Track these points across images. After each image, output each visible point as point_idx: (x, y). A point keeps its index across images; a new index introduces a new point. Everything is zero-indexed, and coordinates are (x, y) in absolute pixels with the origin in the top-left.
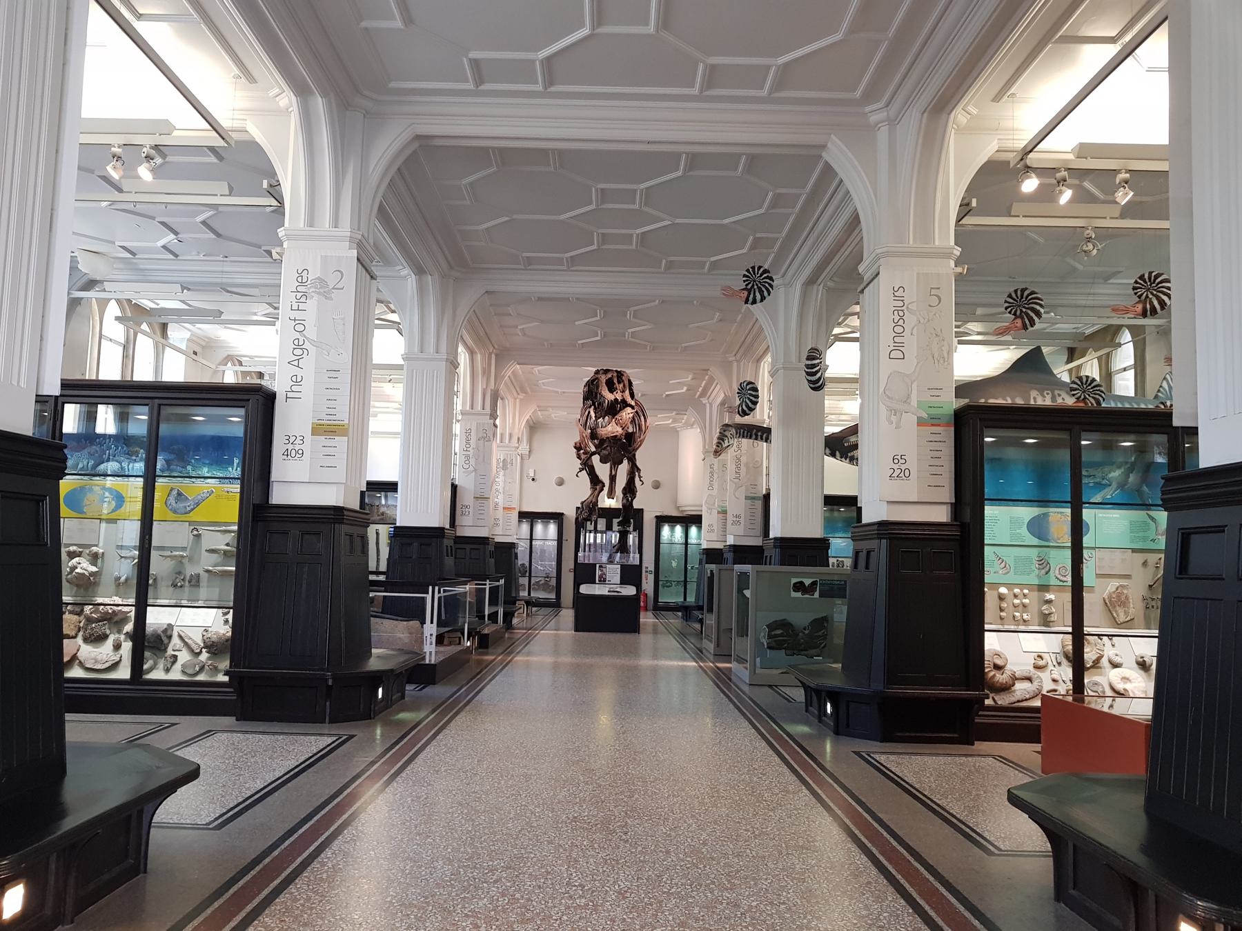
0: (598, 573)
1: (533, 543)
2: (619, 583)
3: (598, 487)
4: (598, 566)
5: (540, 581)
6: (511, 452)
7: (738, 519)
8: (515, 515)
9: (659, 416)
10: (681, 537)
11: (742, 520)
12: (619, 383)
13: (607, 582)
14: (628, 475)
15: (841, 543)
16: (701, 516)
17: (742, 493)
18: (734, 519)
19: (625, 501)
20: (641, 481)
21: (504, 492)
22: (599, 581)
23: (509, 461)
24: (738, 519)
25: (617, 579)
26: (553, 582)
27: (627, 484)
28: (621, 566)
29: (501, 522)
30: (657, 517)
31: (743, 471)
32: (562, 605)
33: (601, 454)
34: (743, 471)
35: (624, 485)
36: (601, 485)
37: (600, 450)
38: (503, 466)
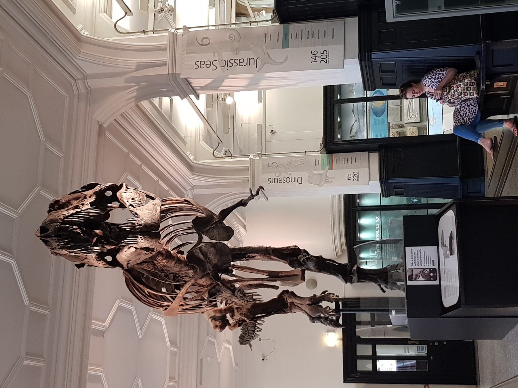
0: (421, 282)
2: (436, 247)
4: (409, 283)
7: (319, 55)
11: (320, 49)
13: (436, 267)
17: (279, 54)
18: (318, 59)
22: (435, 279)
24: (319, 55)
25: (429, 251)
28: (406, 245)
31: (244, 55)
34: (244, 55)
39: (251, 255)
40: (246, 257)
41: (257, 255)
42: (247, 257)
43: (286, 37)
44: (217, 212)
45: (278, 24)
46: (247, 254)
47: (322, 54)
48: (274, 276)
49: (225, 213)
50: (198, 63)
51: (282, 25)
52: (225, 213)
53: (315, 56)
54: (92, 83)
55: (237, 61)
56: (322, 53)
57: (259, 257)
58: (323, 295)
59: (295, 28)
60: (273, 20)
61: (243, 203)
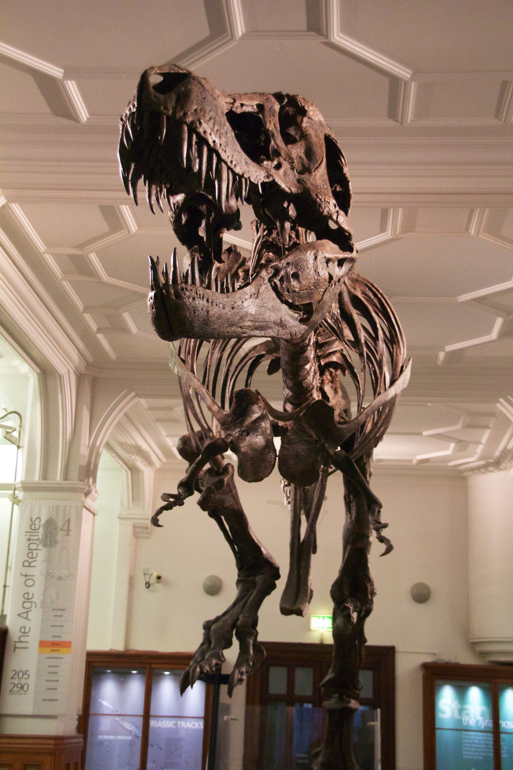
1: (153, 723)
3: (259, 579)
9: (425, 433)
10: (483, 715)
12: (289, 140)
19: (340, 621)
20: (382, 539)
21: (43, 602)
23: (60, 525)
27: (345, 571)
29: (32, 682)
30: (426, 667)
33: (244, 446)
35: (334, 575)
37: (236, 433)
38: (46, 537)
39: (353, 505)
41: (353, 518)
42: (349, 498)
46: (355, 497)
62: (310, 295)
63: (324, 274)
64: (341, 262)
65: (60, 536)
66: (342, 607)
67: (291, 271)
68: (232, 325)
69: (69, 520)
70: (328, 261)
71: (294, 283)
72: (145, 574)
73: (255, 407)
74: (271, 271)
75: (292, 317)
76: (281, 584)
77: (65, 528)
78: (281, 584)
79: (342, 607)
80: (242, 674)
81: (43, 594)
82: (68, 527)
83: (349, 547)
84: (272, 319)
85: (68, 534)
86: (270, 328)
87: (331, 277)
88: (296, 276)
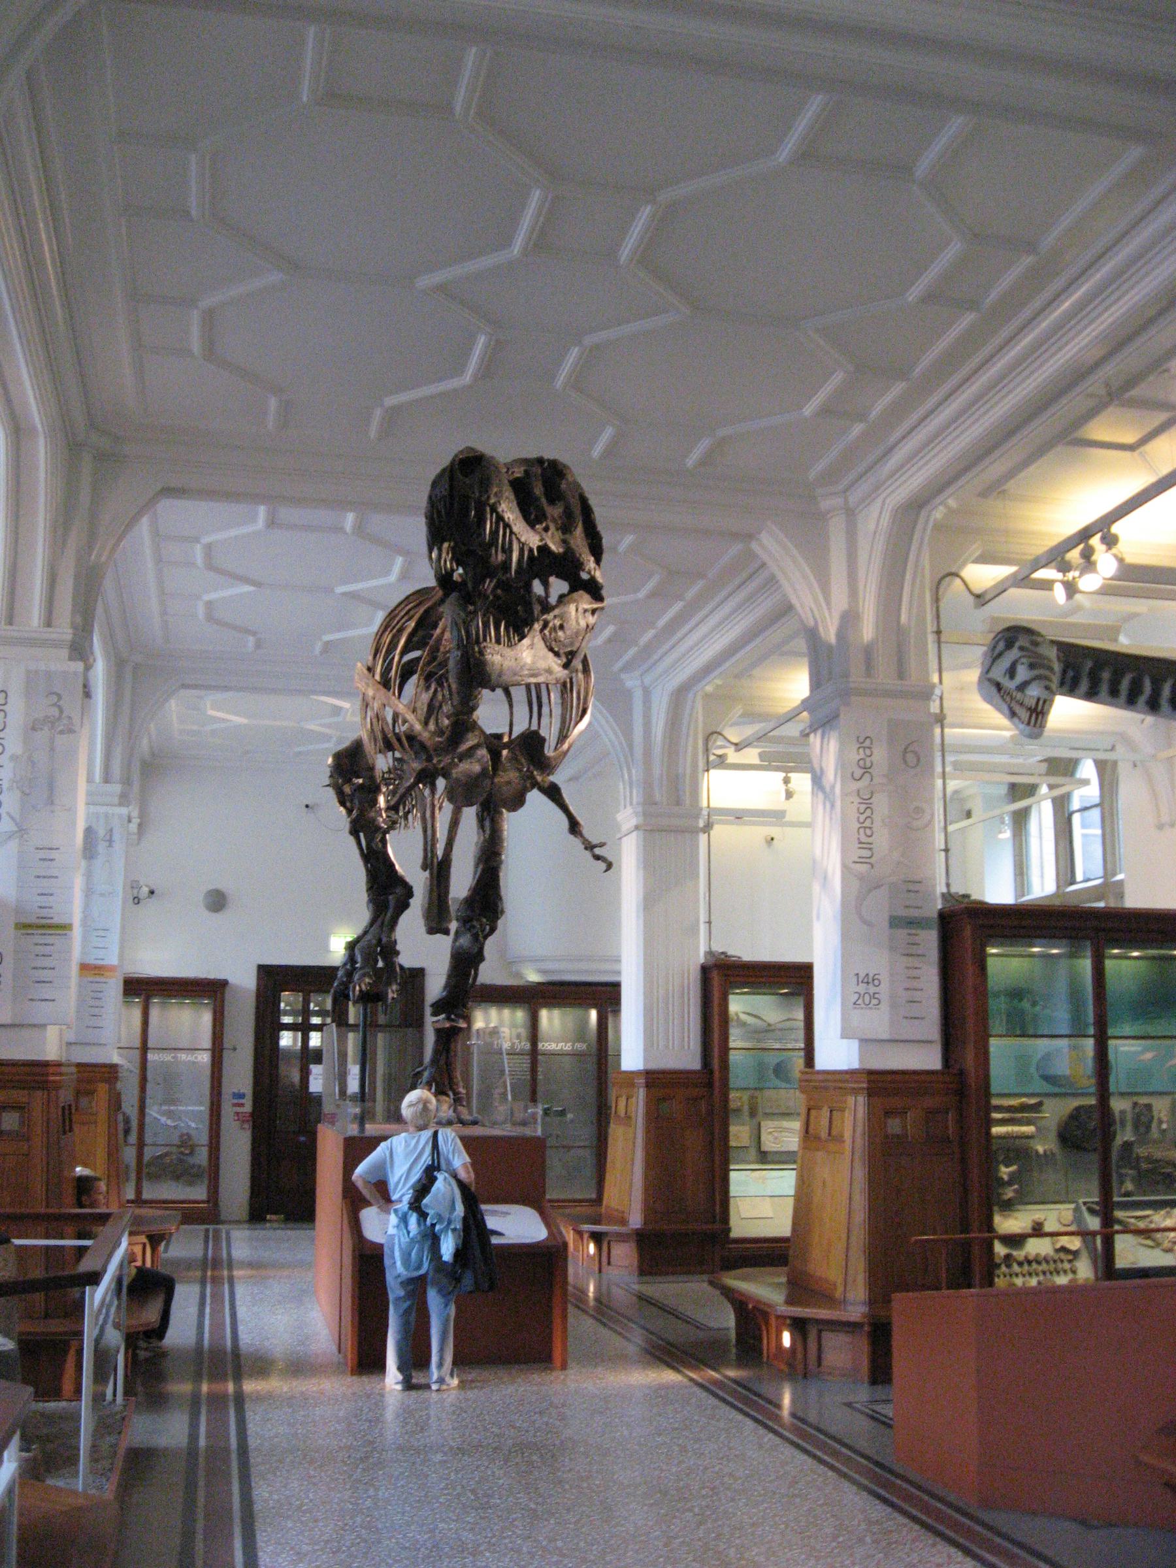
1: (151, 1056)
5: (166, 1154)
6: (110, 810)
7: (872, 989)
8: (113, 989)
11: (884, 989)
14: (476, 866)
15: (1143, 1052)
16: (617, 986)
18: (862, 988)
23: (101, 832)
24: (872, 989)
26: (202, 1157)
32: (222, 1218)
33: (455, 773)
36: (399, 890)
39: (487, 824)
40: (483, 811)
41: (487, 836)
43: (912, 923)
44: (558, 778)
45: (939, 907)
46: (488, 815)
47: (873, 996)
48: (439, 871)
49: (553, 793)
50: (867, 743)
51: (935, 915)
52: (553, 793)
53: (870, 980)
54: (836, 529)
55: (867, 824)
56: (876, 996)
57: (482, 838)
58: (398, 969)
59: (930, 940)
60: (947, 897)
61: (574, 827)
62: (572, 644)
63: (583, 624)
64: (594, 612)
65: (101, 847)
66: (468, 926)
67: (557, 622)
68: (515, 674)
69: (111, 830)
70: (585, 611)
71: (560, 633)
72: (132, 887)
73: (470, 735)
74: (541, 623)
75: (556, 663)
76: (418, 902)
77: (108, 837)
78: (418, 902)
79: (468, 926)
80: (393, 992)
81: (83, 912)
82: (111, 836)
83: (481, 867)
84: (543, 666)
85: (110, 846)
86: (541, 675)
87: (588, 626)
88: (562, 627)
